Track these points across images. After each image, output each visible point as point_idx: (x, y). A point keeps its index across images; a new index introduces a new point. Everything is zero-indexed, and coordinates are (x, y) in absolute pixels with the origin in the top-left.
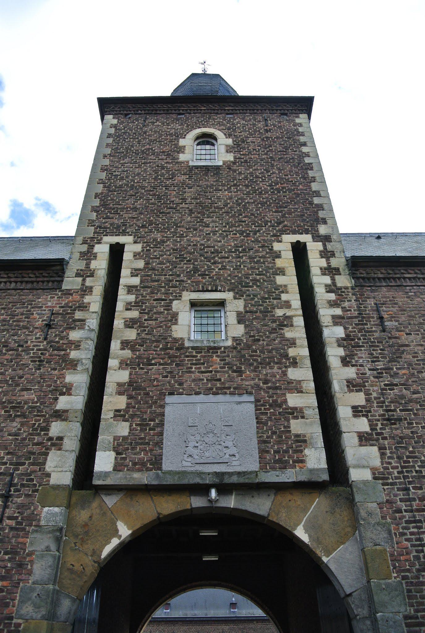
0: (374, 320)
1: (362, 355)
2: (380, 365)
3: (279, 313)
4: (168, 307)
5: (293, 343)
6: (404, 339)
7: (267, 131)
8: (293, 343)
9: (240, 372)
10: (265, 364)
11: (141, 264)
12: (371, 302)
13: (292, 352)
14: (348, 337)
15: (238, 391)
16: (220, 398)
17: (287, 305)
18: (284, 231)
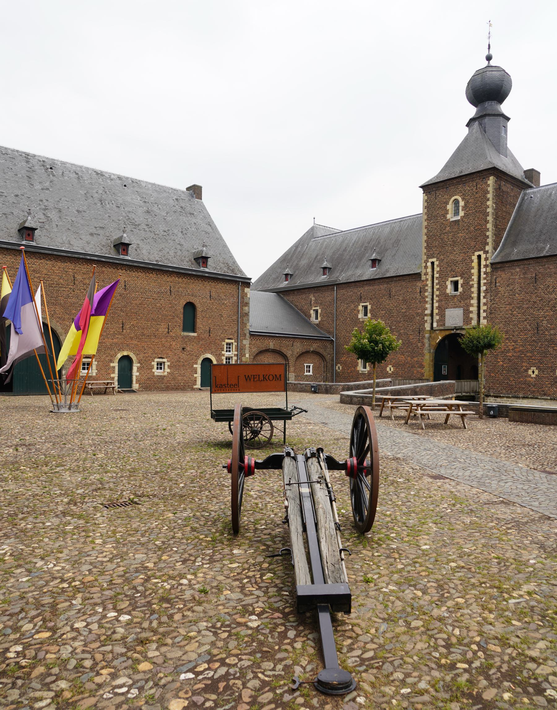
0: (494, 284)
1: (489, 295)
2: (492, 298)
3: (471, 283)
4: (445, 283)
5: (473, 292)
6: (500, 289)
7: (476, 193)
8: (473, 292)
9: (460, 302)
10: (466, 299)
11: (438, 269)
12: (495, 277)
13: (472, 295)
14: (486, 290)
15: (460, 307)
16: (456, 309)
17: (473, 280)
18: (475, 251)
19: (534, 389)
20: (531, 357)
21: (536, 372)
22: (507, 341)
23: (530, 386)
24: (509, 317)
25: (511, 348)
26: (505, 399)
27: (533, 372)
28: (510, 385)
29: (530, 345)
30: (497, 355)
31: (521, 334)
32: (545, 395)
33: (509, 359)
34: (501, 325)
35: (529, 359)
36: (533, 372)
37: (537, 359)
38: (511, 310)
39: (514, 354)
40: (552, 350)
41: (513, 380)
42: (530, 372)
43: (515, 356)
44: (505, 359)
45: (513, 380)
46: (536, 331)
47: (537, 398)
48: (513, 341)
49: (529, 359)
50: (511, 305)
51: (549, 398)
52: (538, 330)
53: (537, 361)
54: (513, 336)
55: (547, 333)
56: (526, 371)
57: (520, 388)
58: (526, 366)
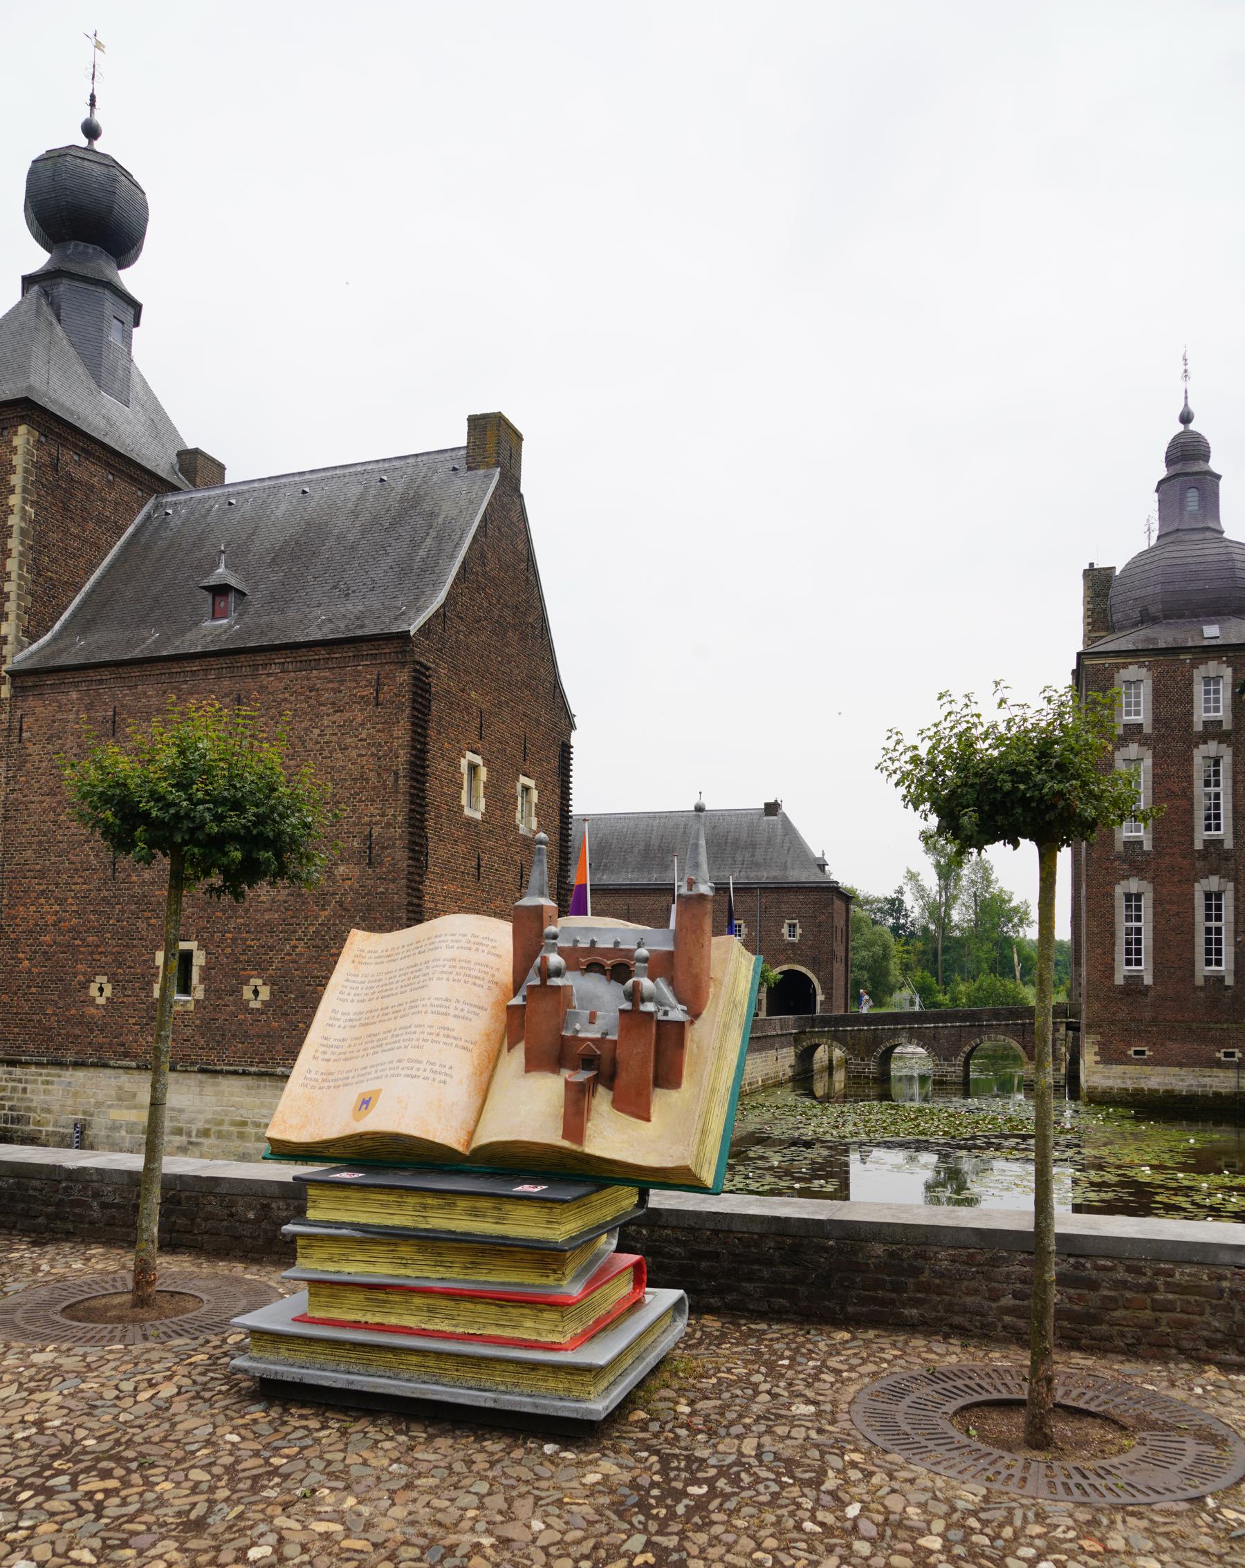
19: (101, 1040)
20: (97, 946)
21: (108, 991)
22: (42, 900)
23: (92, 1031)
24: (49, 830)
25: (51, 919)
26: (33, 1069)
27: (101, 990)
28: (45, 1029)
29: (94, 912)
30: (18, 940)
31: (76, 879)
33: (45, 953)
34: (29, 853)
35: (92, 953)
36: (101, 990)
37: (111, 953)
39: (58, 939)
40: (144, 926)
41: (54, 1014)
42: (93, 990)
43: (59, 945)
44: (35, 952)
45: (54, 1014)
46: (109, 873)
47: (106, 1066)
48: (56, 899)
49: (92, 953)
50: (55, 795)
51: (133, 1064)
52: (114, 870)
53: (109, 959)
54: (57, 884)
55: (134, 878)
56: (85, 986)
57: (68, 1035)
58: (84, 974)
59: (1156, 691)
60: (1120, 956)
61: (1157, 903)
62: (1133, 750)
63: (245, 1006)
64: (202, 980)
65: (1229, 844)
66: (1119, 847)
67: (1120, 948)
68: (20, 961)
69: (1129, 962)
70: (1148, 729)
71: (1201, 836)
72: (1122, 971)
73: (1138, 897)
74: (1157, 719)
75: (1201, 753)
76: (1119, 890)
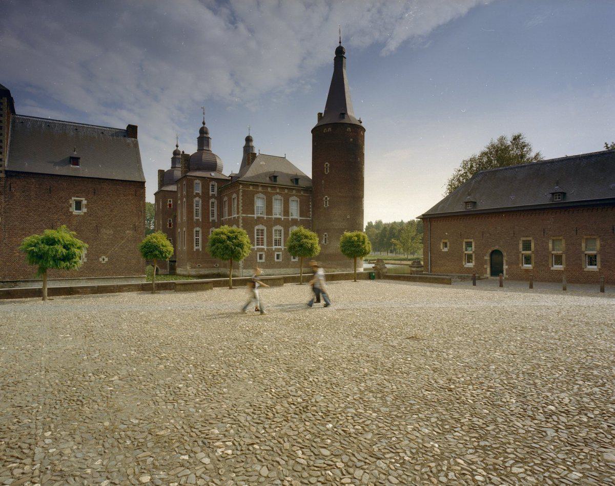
32: (60, 277)
38: (27, 211)
59: (202, 186)
60: (195, 245)
61: (202, 233)
62: (197, 199)
63: (100, 263)
64: (86, 257)
65: (216, 221)
66: (195, 220)
67: (195, 243)
68: (15, 253)
69: (196, 246)
70: (201, 195)
71: (211, 219)
72: (195, 248)
73: (198, 232)
74: (202, 193)
75: (212, 200)
76: (195, 230)
